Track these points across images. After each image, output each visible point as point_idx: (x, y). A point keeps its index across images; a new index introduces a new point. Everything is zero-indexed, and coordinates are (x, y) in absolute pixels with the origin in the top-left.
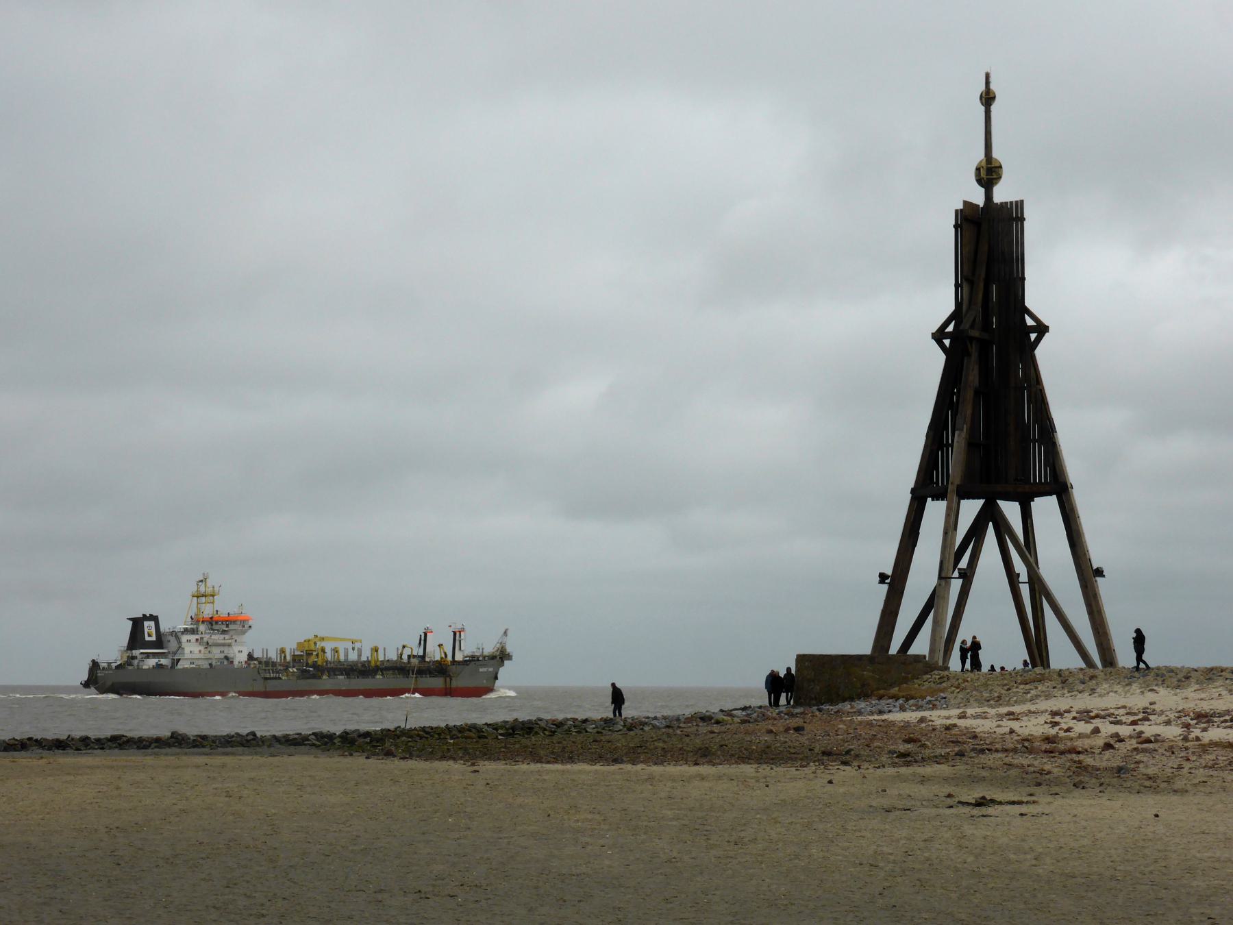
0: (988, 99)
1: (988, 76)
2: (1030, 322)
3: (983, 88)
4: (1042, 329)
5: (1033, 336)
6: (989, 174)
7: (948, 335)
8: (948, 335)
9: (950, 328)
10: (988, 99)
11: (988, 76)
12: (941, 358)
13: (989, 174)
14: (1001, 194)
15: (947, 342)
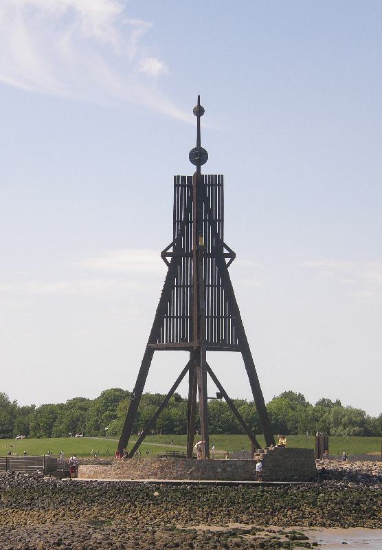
0: (199, 111)
1: (199, 97)
2: (225, 251)
3: (196, 104)
4: (232, 255)
5: (227, 260)
6: (199, 156)
7: (169, 255)
8: (169, 255)
9: (171, 250)
10: (199, 111)
11: (199, 97)
12: (166, 269)
13: (199, 156)
14: (206, 170)
15: (169, 259)
